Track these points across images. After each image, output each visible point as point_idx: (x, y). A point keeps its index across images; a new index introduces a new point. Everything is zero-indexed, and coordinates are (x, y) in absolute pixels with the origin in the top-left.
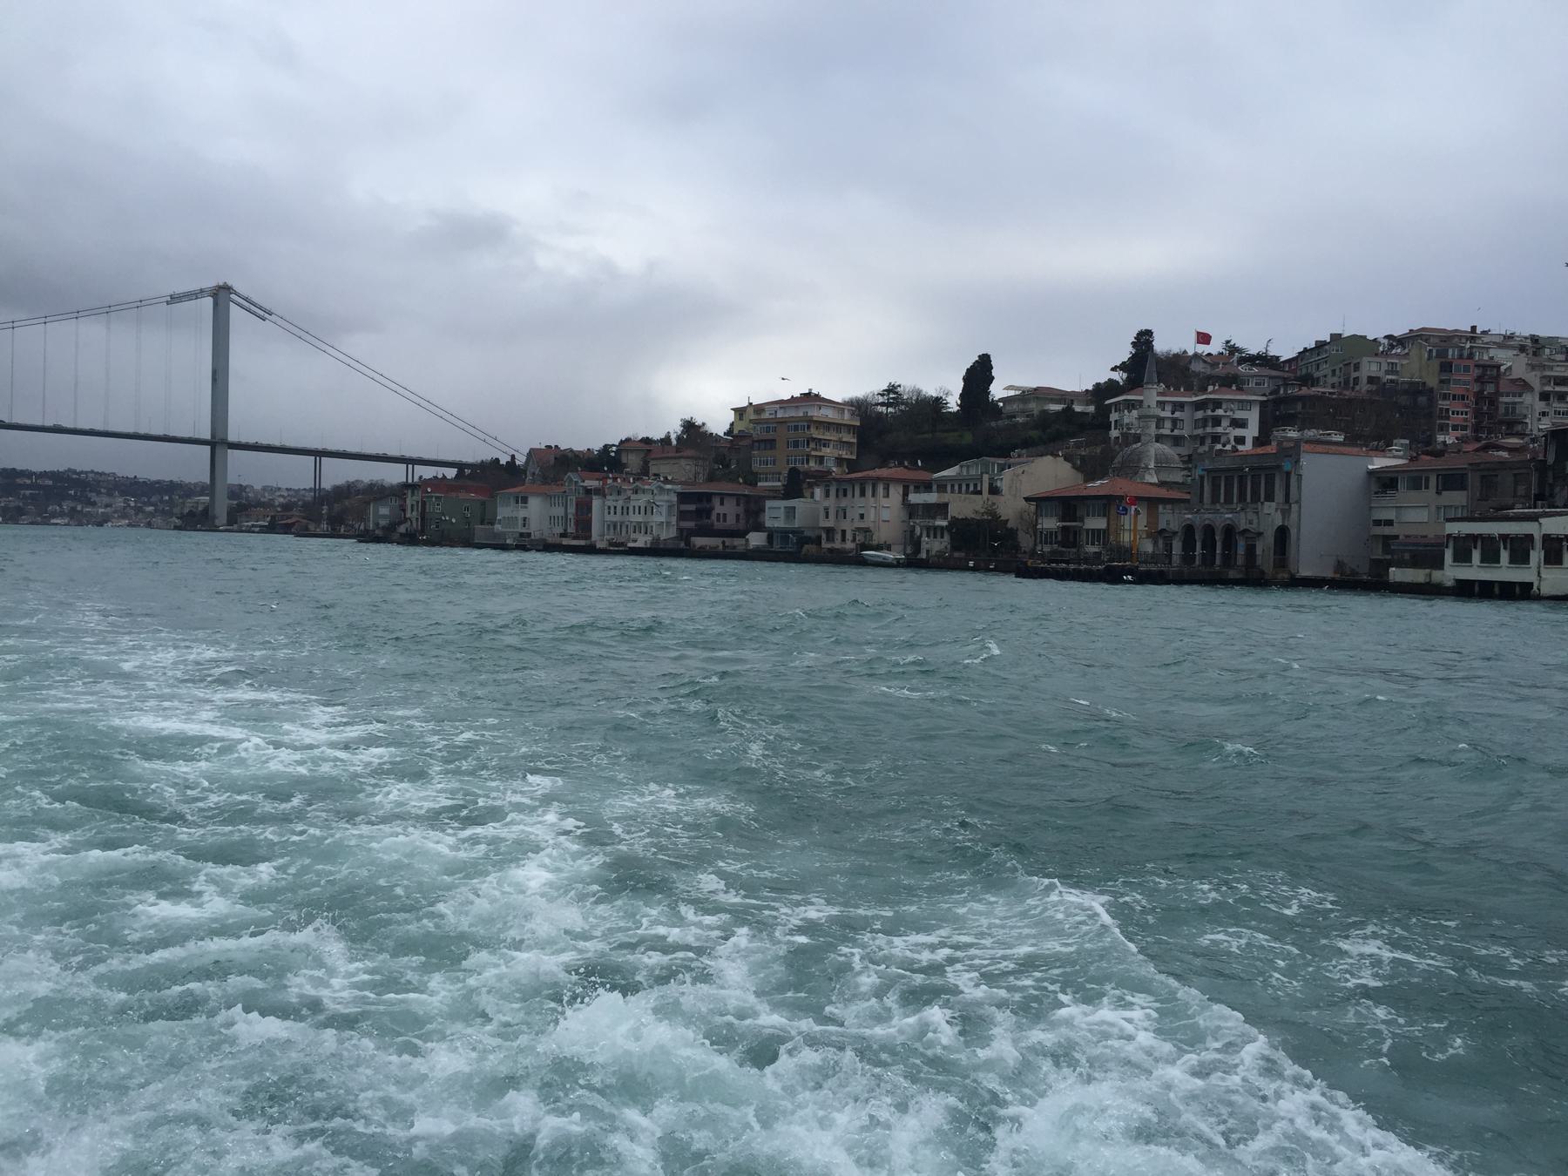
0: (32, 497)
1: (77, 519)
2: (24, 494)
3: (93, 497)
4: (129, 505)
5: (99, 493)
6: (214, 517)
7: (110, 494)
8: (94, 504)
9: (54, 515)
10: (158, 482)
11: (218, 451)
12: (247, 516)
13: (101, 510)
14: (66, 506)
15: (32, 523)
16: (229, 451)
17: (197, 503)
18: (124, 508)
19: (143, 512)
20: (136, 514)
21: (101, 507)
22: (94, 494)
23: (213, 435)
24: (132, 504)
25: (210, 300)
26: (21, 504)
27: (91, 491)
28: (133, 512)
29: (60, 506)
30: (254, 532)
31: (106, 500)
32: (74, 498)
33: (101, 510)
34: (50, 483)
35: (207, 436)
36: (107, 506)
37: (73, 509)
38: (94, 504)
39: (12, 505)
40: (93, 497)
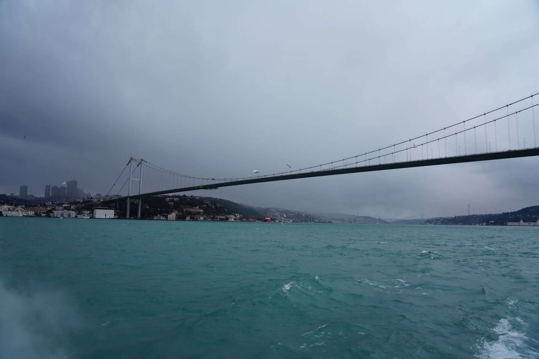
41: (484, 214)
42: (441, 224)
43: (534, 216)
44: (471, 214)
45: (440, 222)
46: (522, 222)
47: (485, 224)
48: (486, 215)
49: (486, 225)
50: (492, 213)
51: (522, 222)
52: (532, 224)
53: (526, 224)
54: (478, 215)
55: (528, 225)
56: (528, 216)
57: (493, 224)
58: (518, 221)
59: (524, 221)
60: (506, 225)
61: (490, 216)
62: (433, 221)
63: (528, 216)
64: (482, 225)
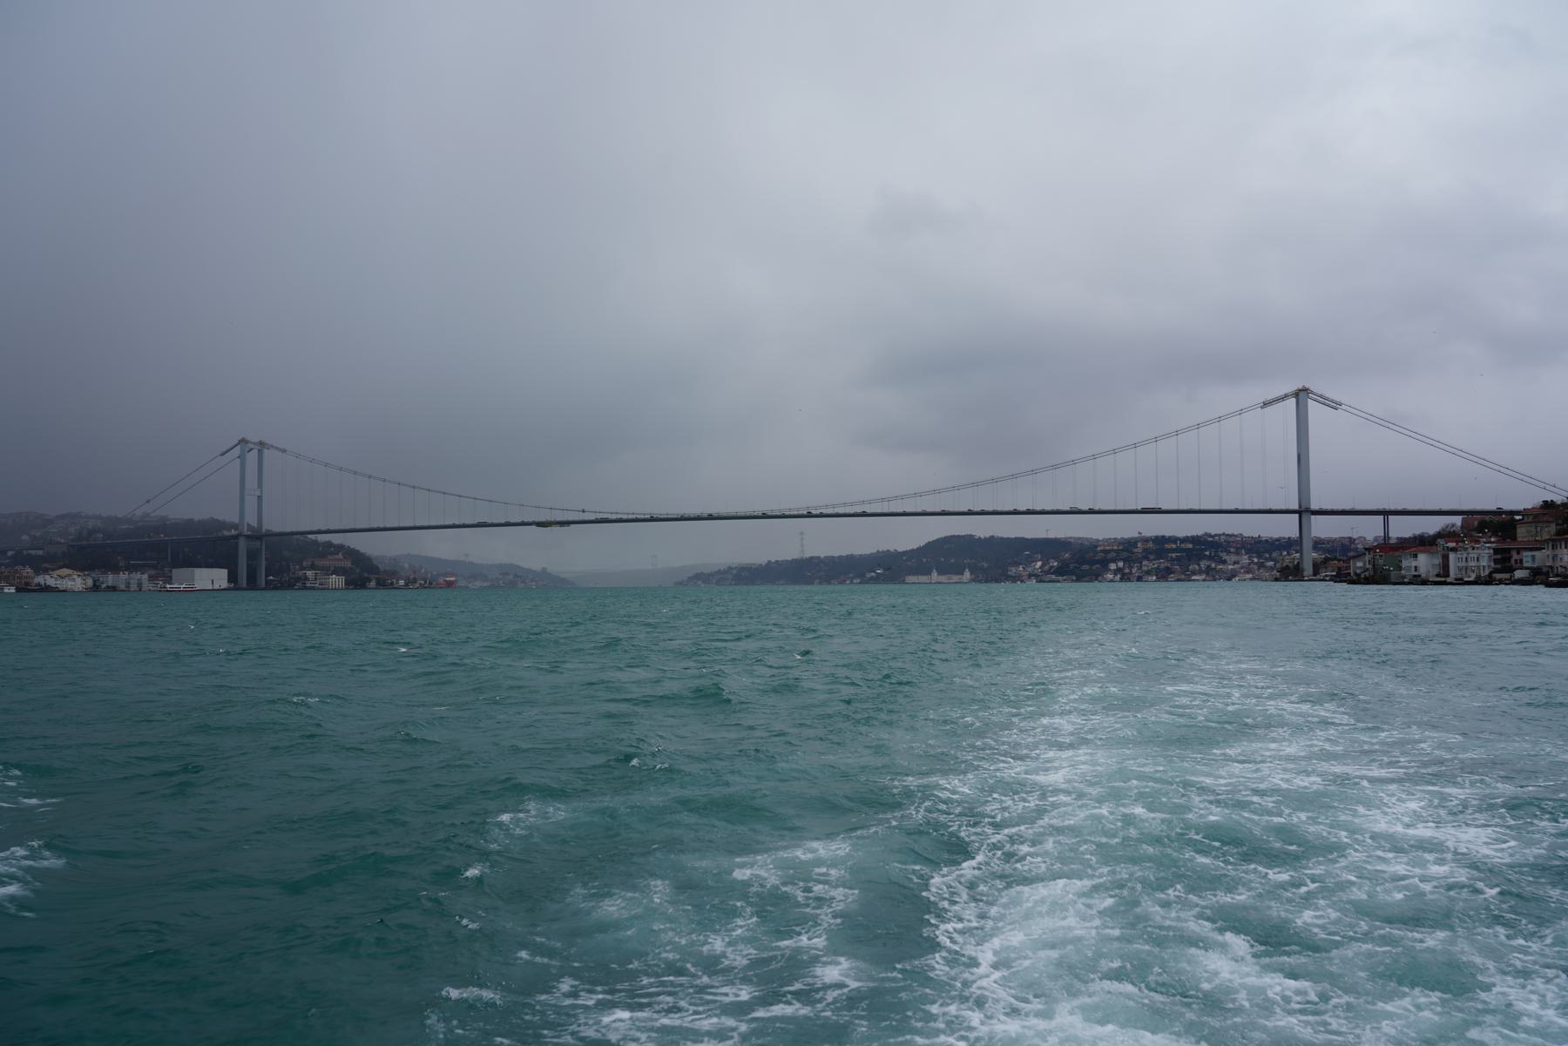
0: (1178, 559)
1: (1212, 575)
2: (1171, 557)
3: (1224, 556)
4: (1253, 562)
5: (1229, 552)
6: (1303, 571)
7: (1237, 553)
8: (1224, 562)
9: (1194, 573)
10: (1278, 540)
11: (1305, 516)
12: (1326, 568)
13: (1230, 567)
14: (1204, 564)
15: (1178, 580)
16: (1313, 517)
17: (1294, 559)
18: (1250, 564)
19: (1265, 567)
20: (1259, 569)
21: (1230, 564)
22: (1225, 554)
23: (1300, 507)
24: (1256, 560)
25: (1293, 400)
26: (1169, 565)
27: (1222, 551)
28: (1256, 567)
29: (1199, 565)
30: (1326, 581)
31: (1234, 558)
32: (1210, 558)
33: (1230, 567)
34: (1190, 546)
35: (1296, 507)
36: (1235, 563)
37: (1209, 566)
38: (1224, 562)
39: (1162, 566)
40: (1224, 556)
41: (836, 555)
42: (735, 584)
43: (952, 561)
44: (808, 555)
45: (730, 576)
46: (936, 574)
47: (858, 581)
48: (840, 557)
49: (860, 583)
50: (855, 553)
51: (935, 574)
52: (955, 578)
53: (943, 578)
54: (822, 556)
55: (947, 581)
56: (943, 559)
57: (877, 580)
58: (929, 573)
59: (939, 574)
60: (904, 582)
61: (850, 558)
62: (711, 575)
63: (943, 559)
64: (852, 583)
